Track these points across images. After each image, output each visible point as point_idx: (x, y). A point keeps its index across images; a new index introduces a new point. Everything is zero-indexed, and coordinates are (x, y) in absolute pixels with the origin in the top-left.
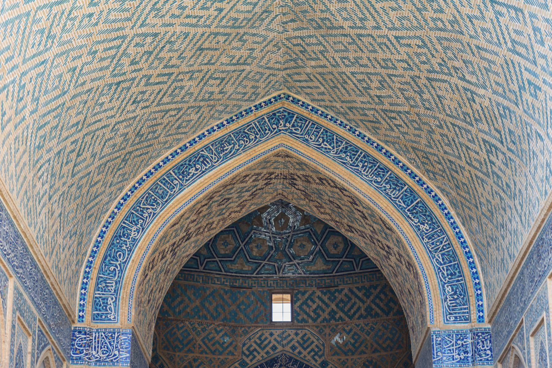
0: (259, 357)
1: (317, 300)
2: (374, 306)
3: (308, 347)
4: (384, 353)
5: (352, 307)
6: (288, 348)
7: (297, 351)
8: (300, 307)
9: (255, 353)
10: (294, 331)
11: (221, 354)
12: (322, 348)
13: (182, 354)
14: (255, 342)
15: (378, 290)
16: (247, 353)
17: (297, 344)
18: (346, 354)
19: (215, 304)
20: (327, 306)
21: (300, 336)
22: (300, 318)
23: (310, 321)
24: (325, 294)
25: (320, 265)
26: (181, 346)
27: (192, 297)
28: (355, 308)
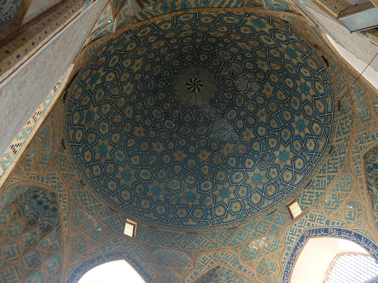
0: (295, 240)
1: (307, 194)
2: (330, 174)
3: (315, 220)
4: (351, 193)
5: (322, 183)
6: (306, 227)
7: (311, 225)
8: (302, 203)
9: (292, 239)
10: (305, 216)
11: (276, 249)
12: (322, 215)
13: (256, 260)
14: (290, 234)
15: (327, 165)
16: (288, 242)
17: (309, 222)
18: (335, 209)
19: (262, 227)
20: (313, 193)
21: (309, 216)
22: (304, 208)
23: (309, 206)
24: (309, 188)
25: (299, 178)
26: (254, 256)
27: (250, 229)
28: (323, 183)
